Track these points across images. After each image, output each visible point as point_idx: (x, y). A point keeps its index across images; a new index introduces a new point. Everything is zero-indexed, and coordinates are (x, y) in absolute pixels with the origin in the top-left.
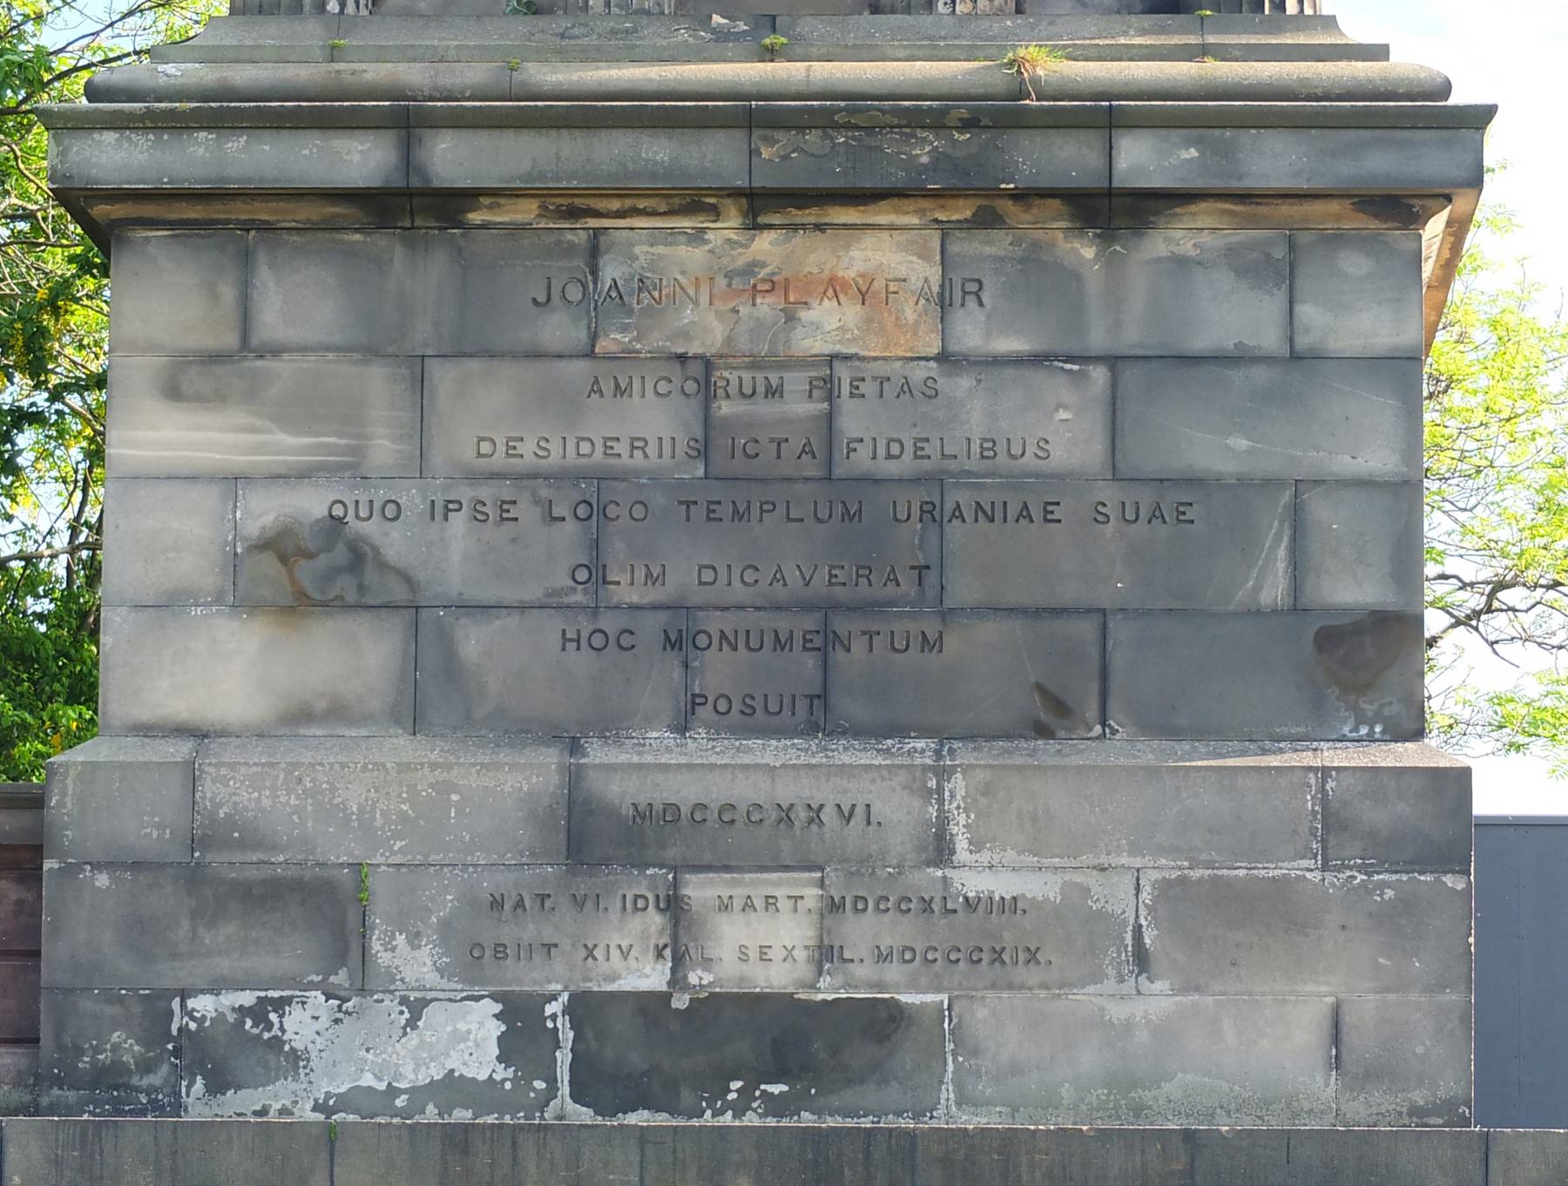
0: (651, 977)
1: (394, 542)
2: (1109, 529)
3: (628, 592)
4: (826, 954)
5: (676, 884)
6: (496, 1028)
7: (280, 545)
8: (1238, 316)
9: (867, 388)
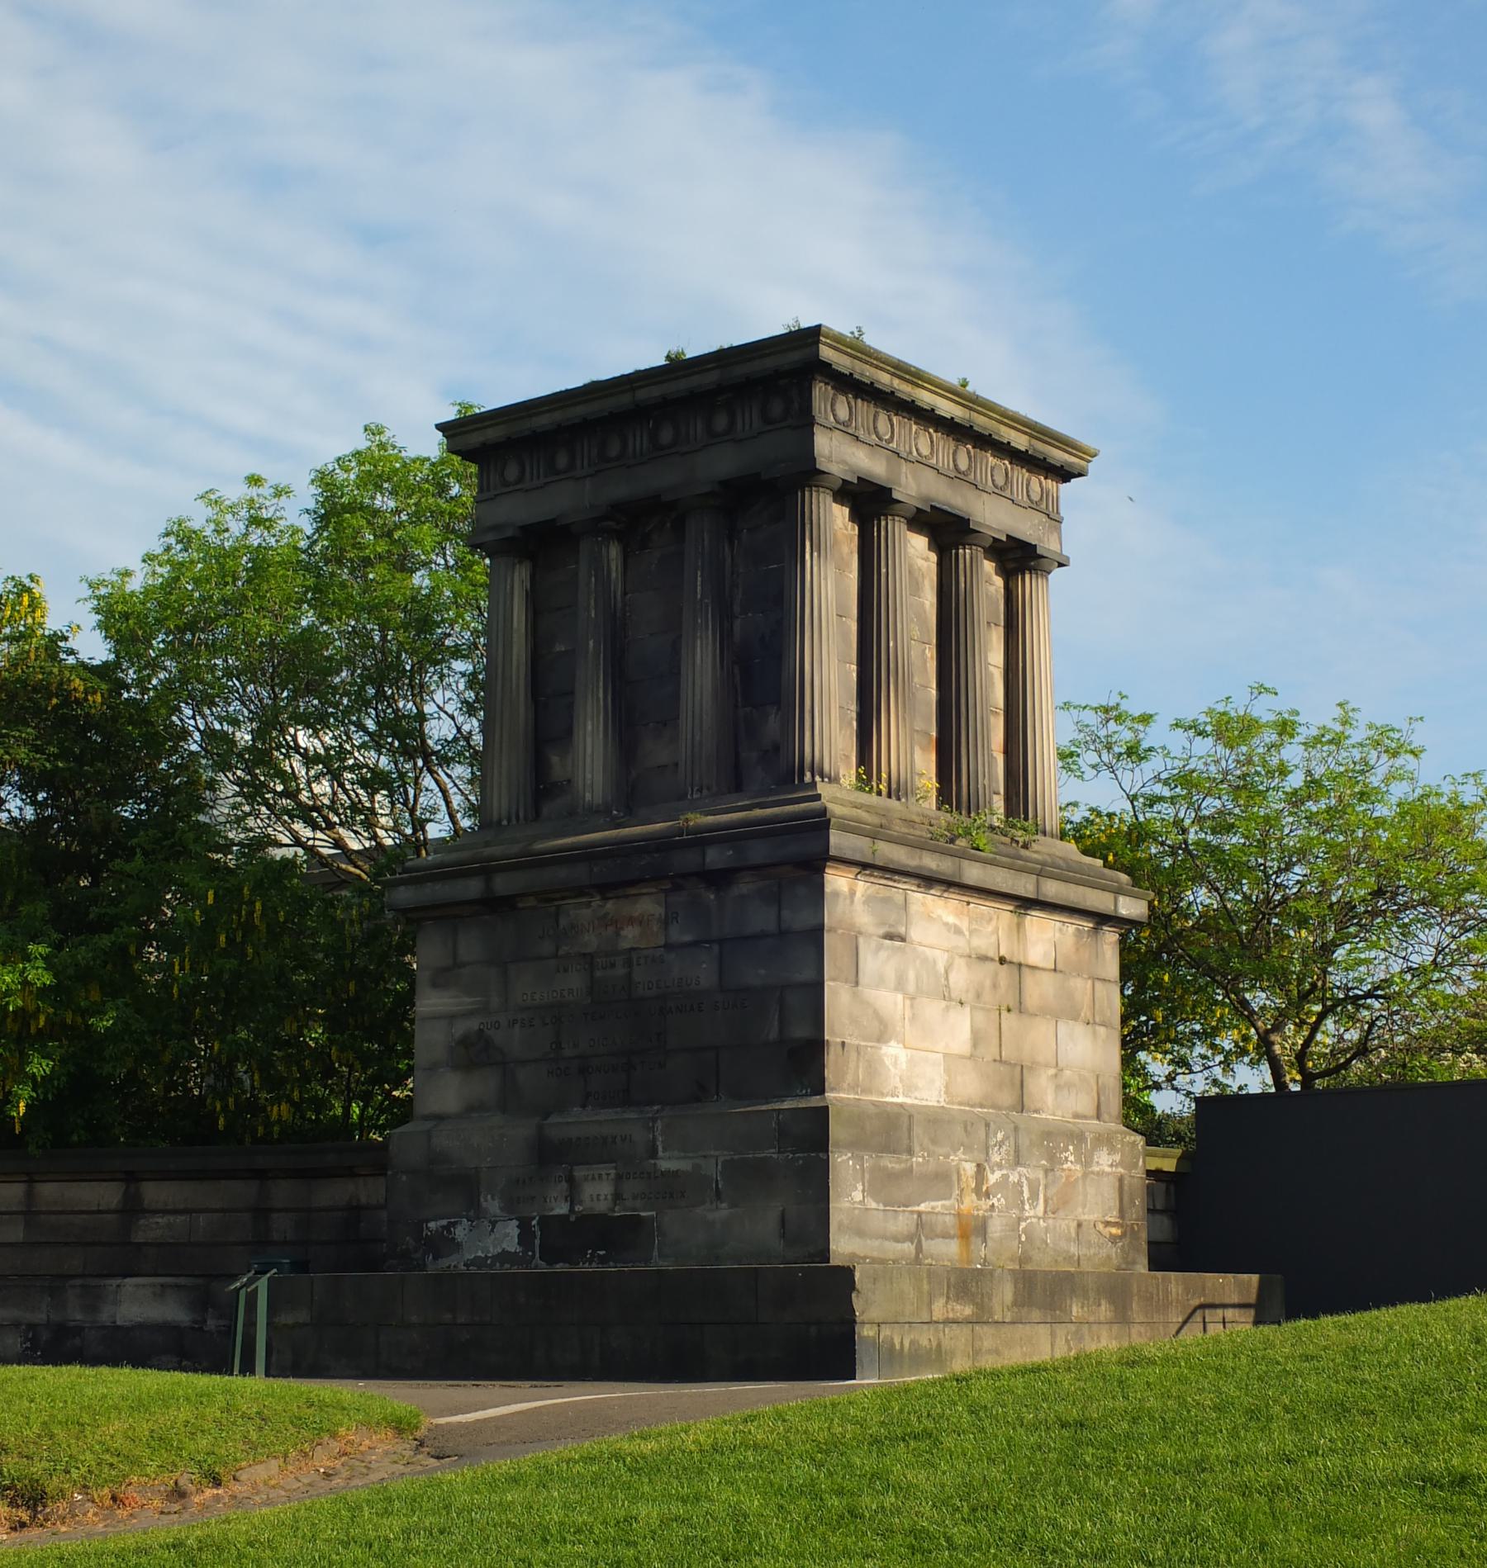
0: (562, 1209)
3: (568, 1052)
4: (618, 1197)
5: (571, 1171)
6: (517, 1231)
7: (465, 1042)
8: (761, 919)
9: (642, 961)
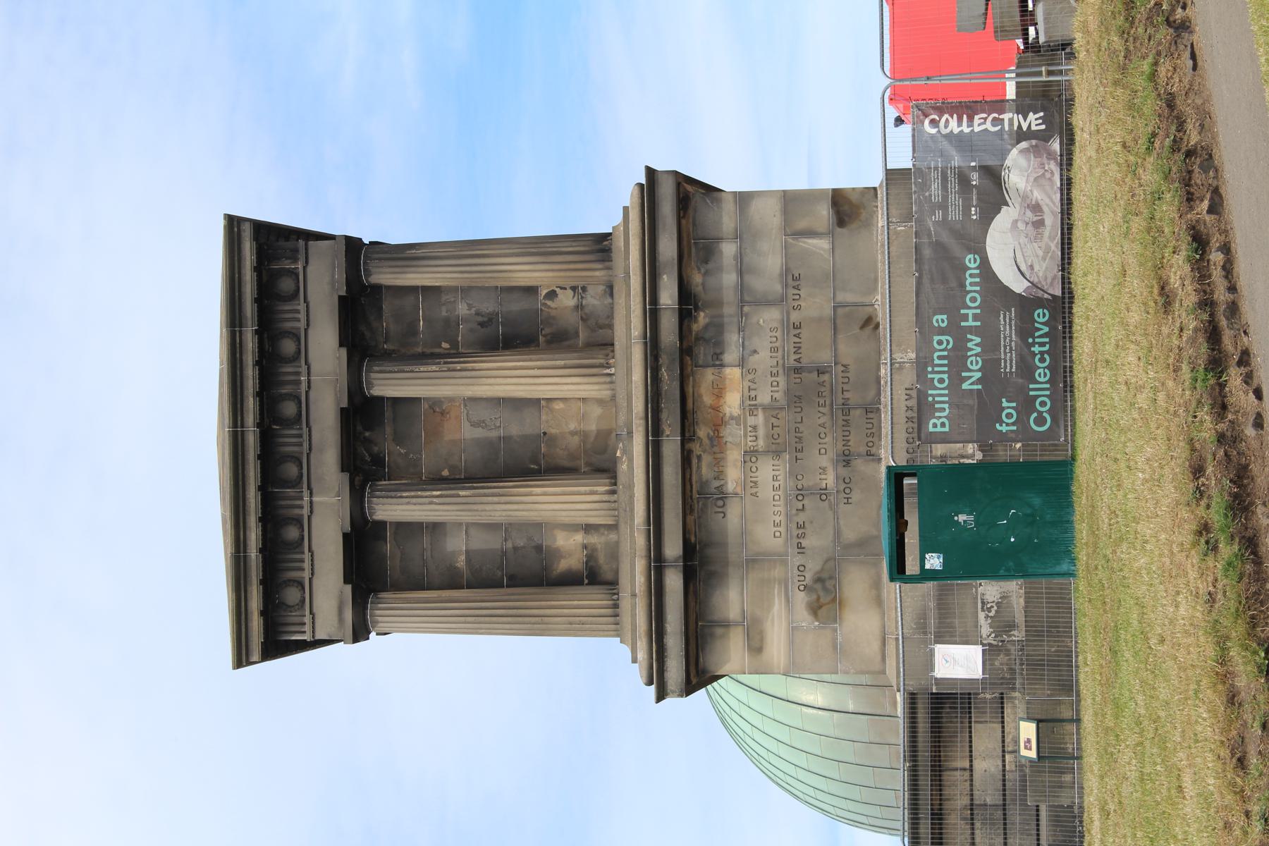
1: (813, 567)
2: (803, 304)
7: (815, 609)
